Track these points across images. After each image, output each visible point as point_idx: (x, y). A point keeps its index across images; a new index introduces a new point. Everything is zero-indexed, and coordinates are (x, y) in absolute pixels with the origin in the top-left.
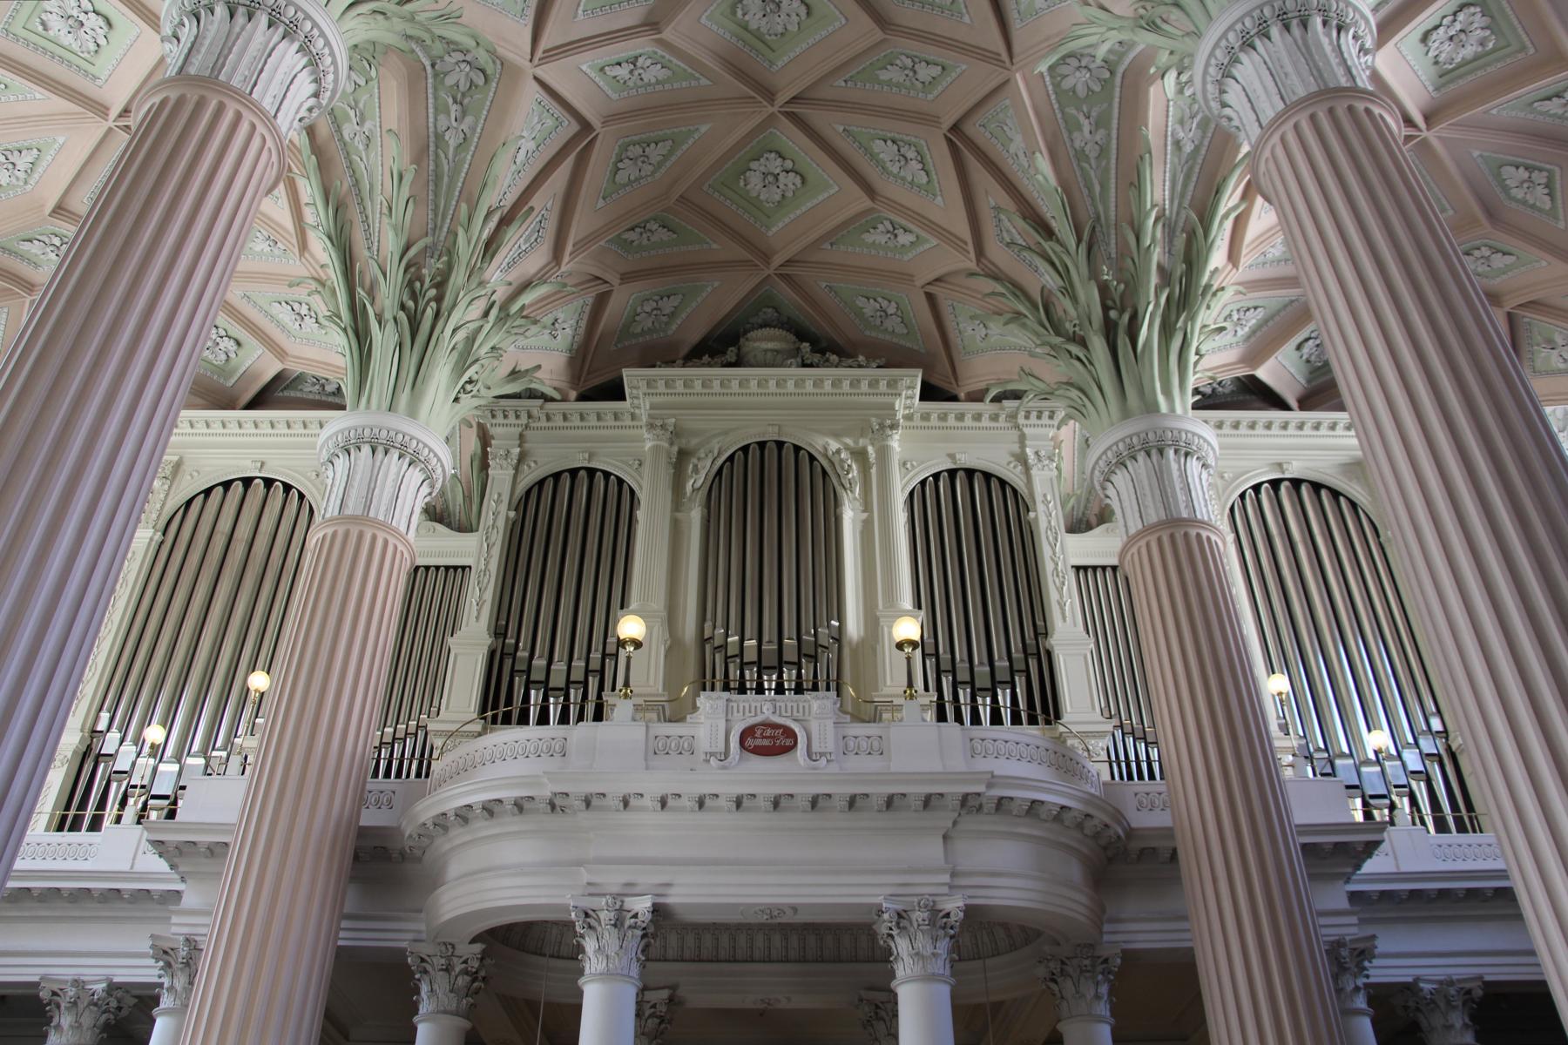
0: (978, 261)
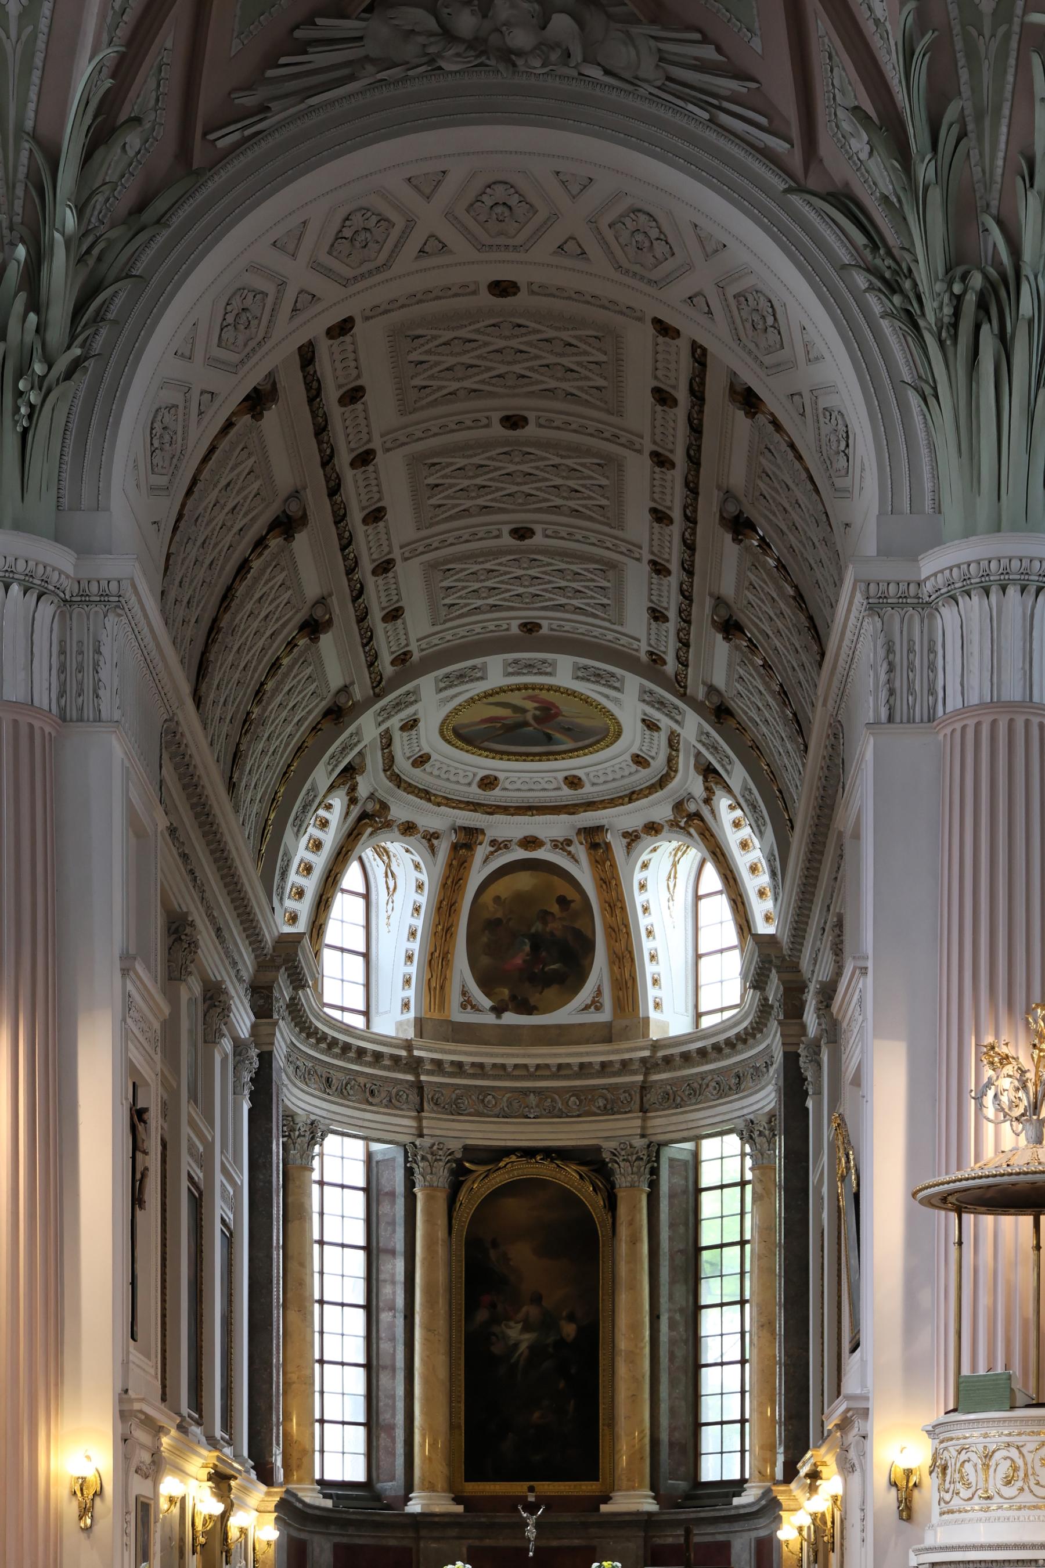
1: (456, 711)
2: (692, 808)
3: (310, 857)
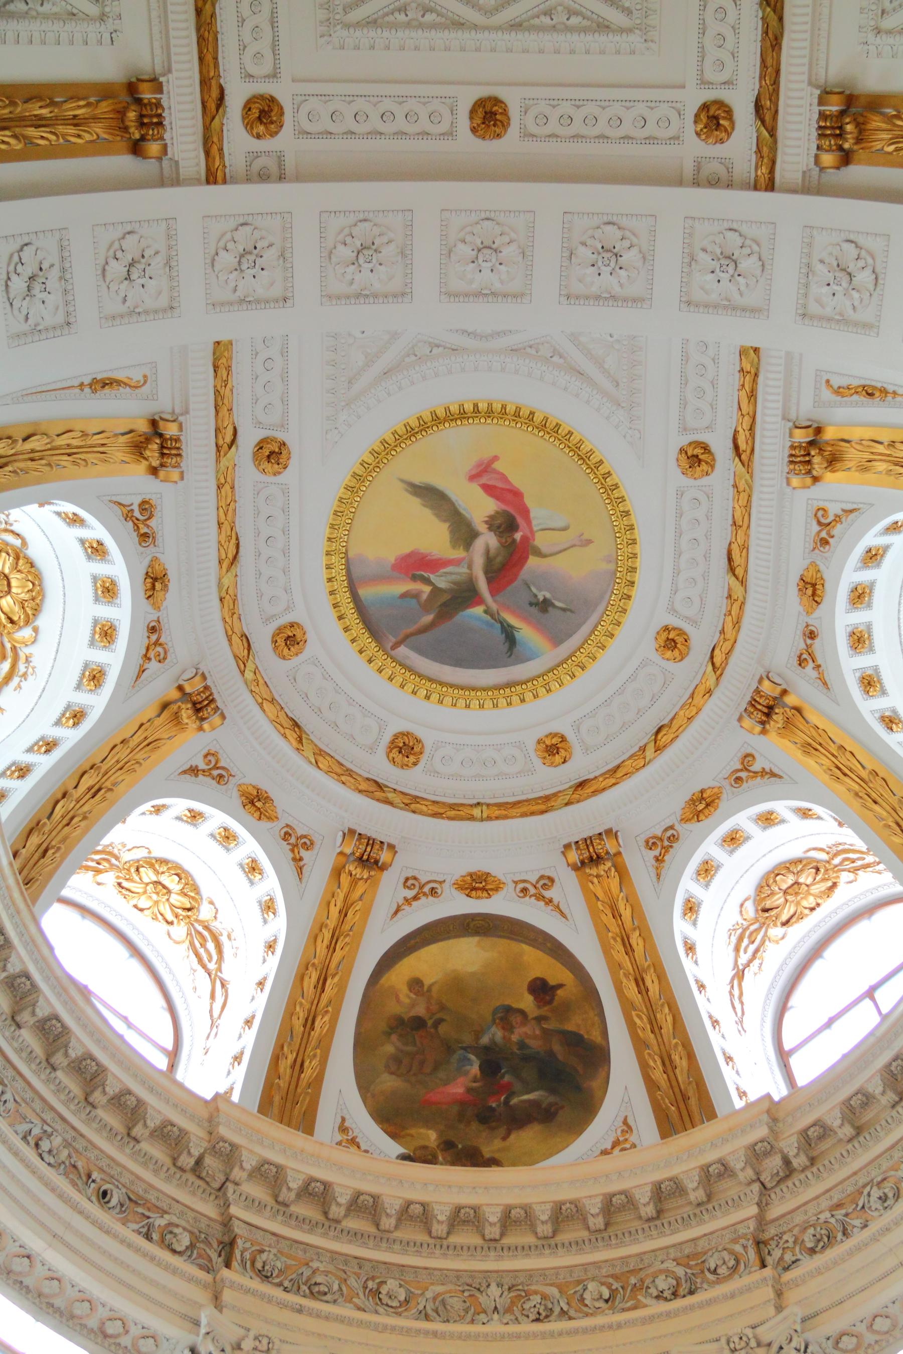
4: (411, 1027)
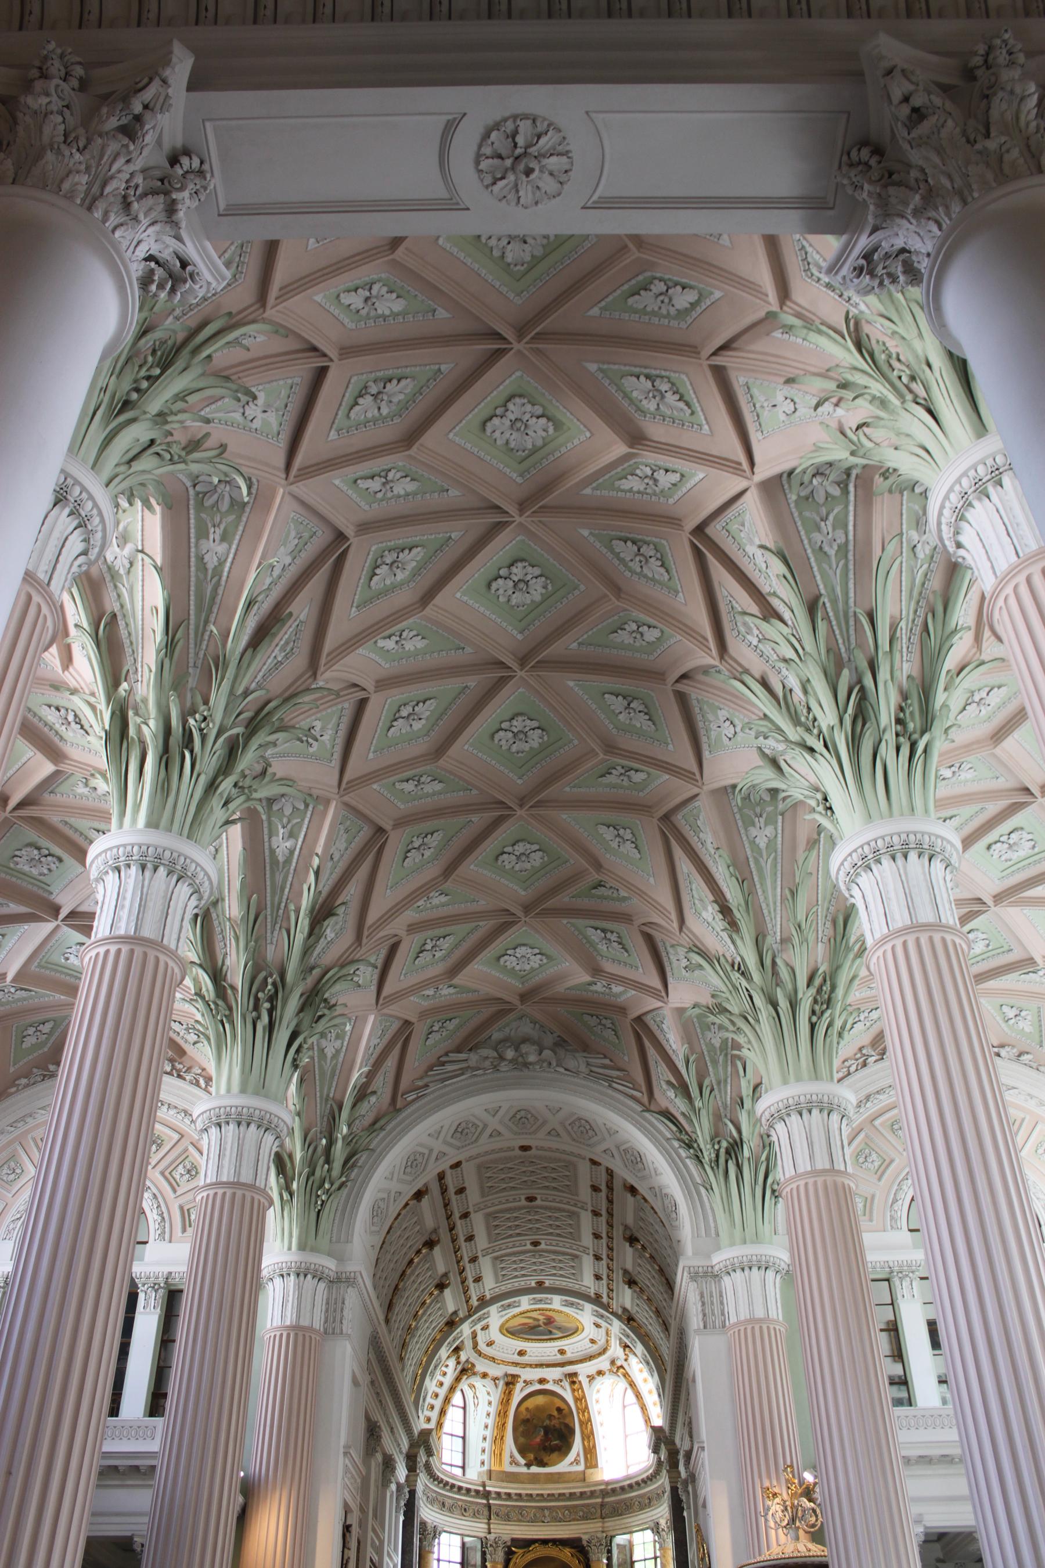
0: (722, 658)
1: (507, 1321)
2: (619, 1363)
3: (437, 1390)
4: (526, 1421)
